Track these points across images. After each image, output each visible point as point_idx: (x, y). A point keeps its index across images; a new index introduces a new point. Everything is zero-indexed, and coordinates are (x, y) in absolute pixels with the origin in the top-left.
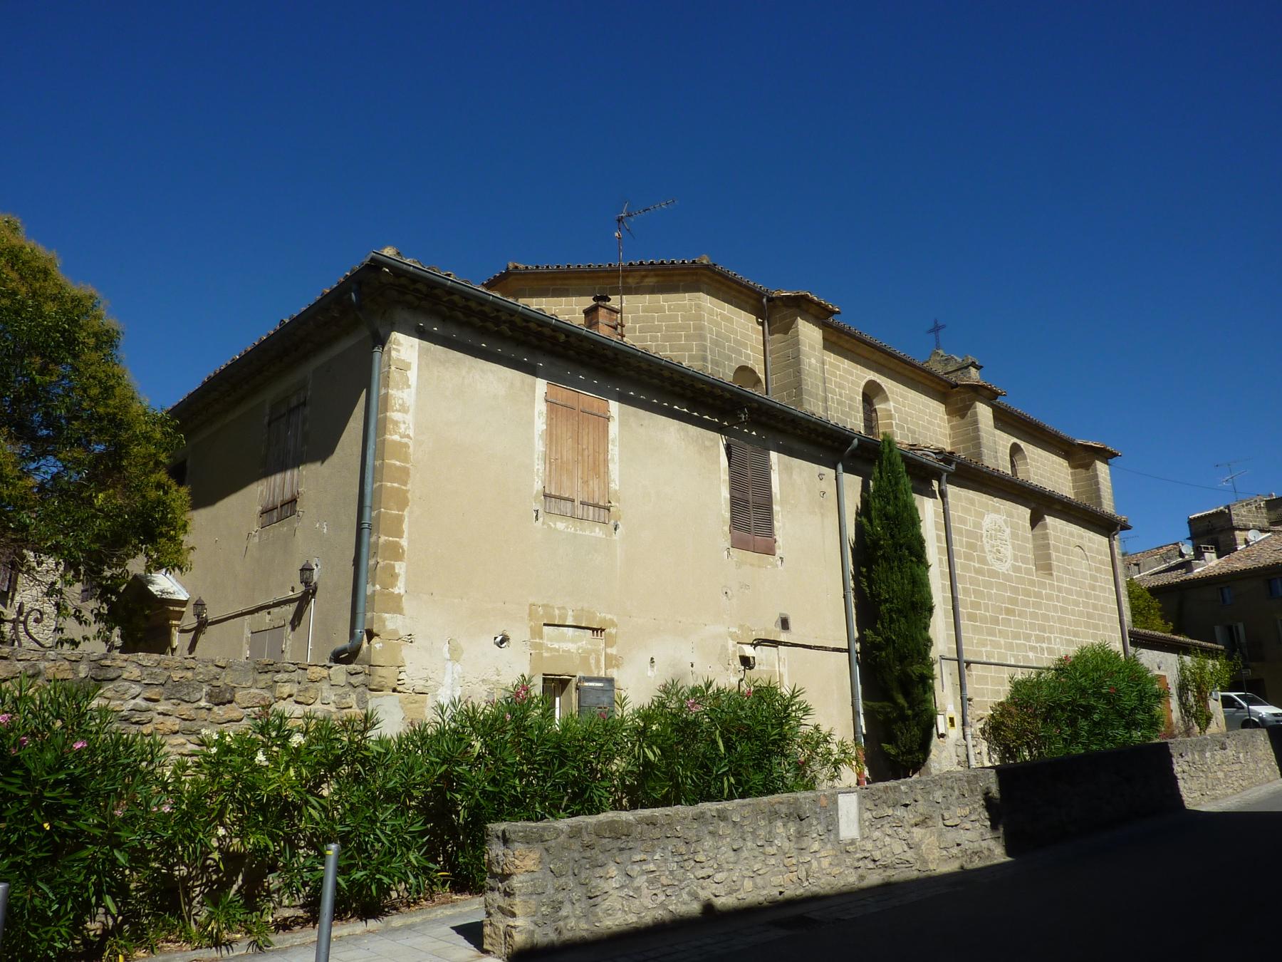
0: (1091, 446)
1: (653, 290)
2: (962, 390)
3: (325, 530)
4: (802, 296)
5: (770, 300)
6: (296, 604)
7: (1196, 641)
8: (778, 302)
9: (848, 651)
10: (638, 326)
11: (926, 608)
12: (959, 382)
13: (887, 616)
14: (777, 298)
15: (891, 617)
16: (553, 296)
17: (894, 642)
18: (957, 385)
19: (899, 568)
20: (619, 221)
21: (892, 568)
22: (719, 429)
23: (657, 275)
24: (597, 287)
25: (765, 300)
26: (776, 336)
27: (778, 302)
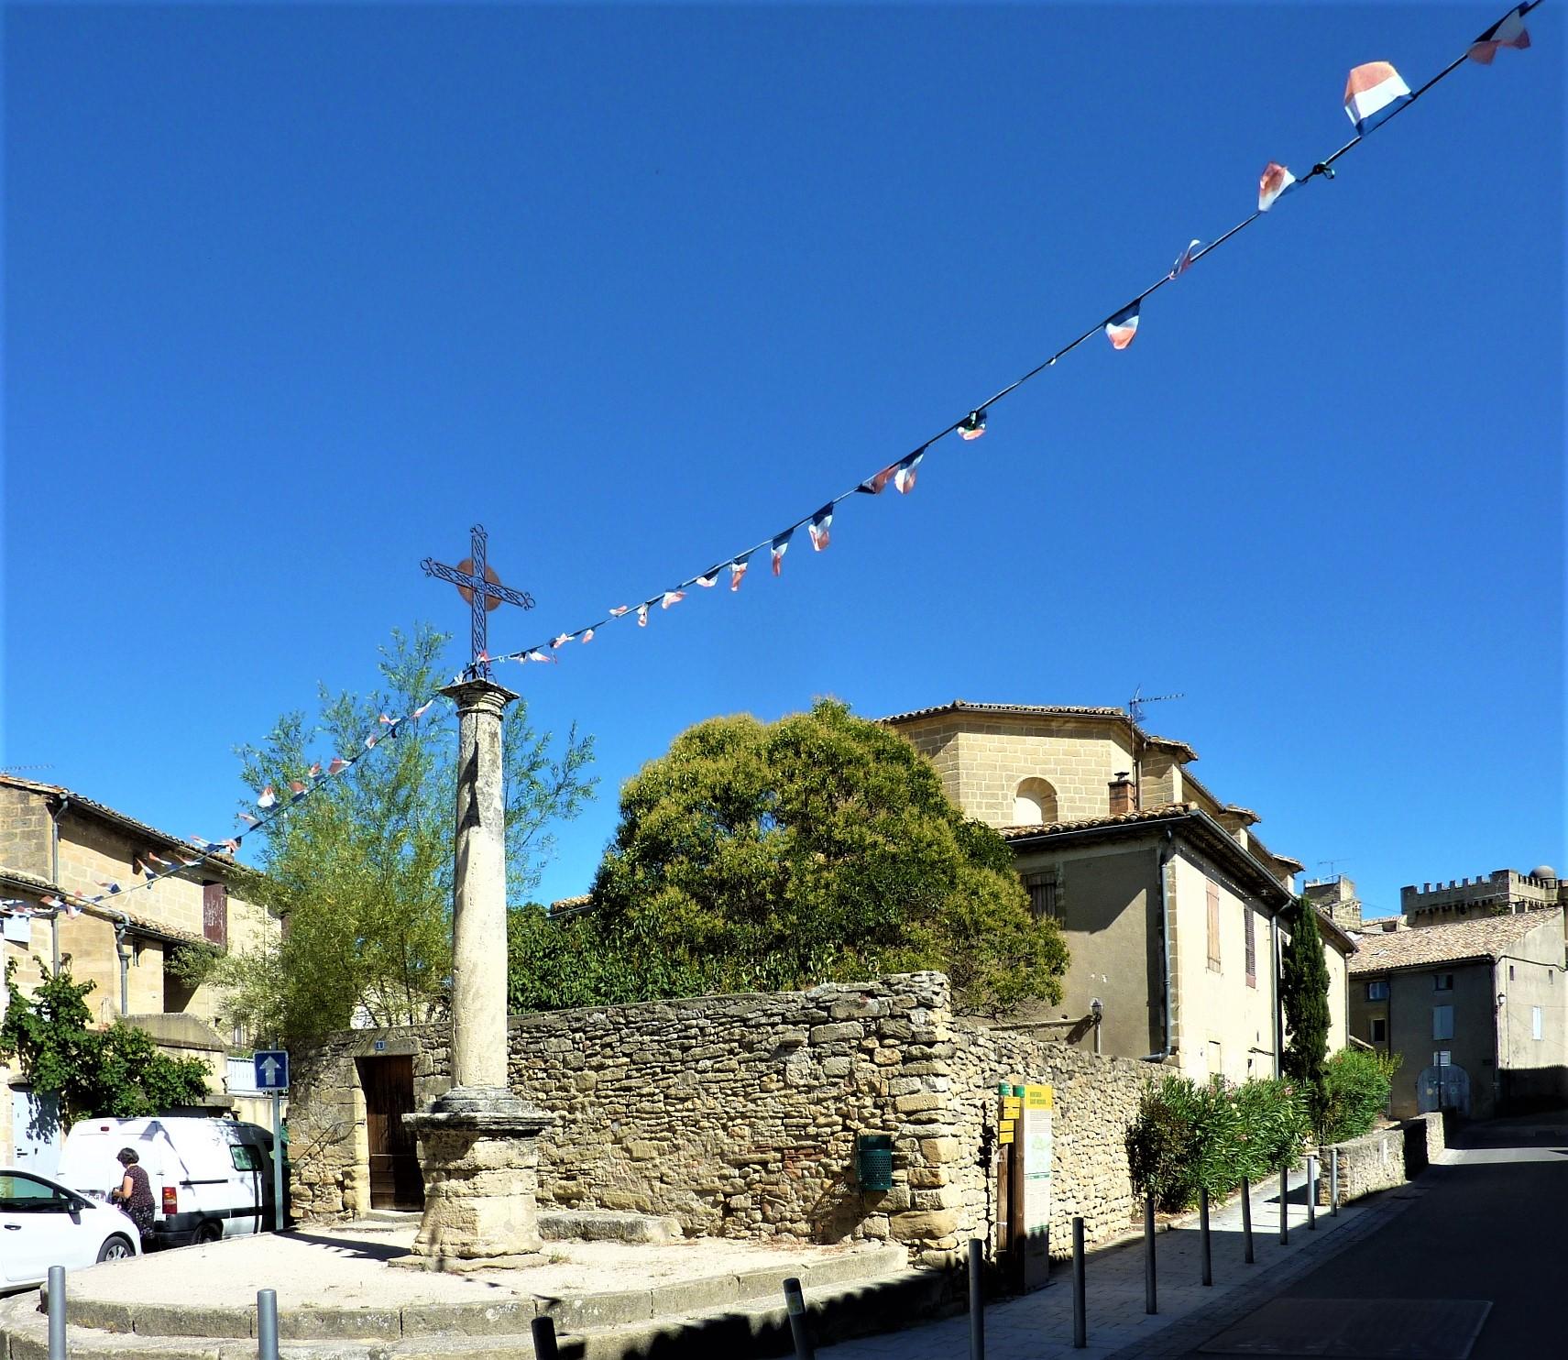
0: (1286, 862)
1: (1071, 735)
2: (1229, 816)
3: (1105, 980)
4: (1181, 747)
5: (1149, 744)
6: (1073, 1027)
7: (1364, 1043)
8: (1155, 748)
9: (1273, 1055)
10: (1059, 768)
11: (1325, 1023)
12: (1227, 809)
13: (1305, 1031)
14: (1154, 743)
15: (1308, 1032)
16: (987, 733)
17: (1309, 1049)
18: (1225, 811)
19: (1315, 997)
20: (1131, 704)
21: (1309, 997)
22: (1242, 898)
23: (1077, 722)
24: (1025, 727)
25: (1145, 745)
26: (1148, 778)
27: (1155, 748)
